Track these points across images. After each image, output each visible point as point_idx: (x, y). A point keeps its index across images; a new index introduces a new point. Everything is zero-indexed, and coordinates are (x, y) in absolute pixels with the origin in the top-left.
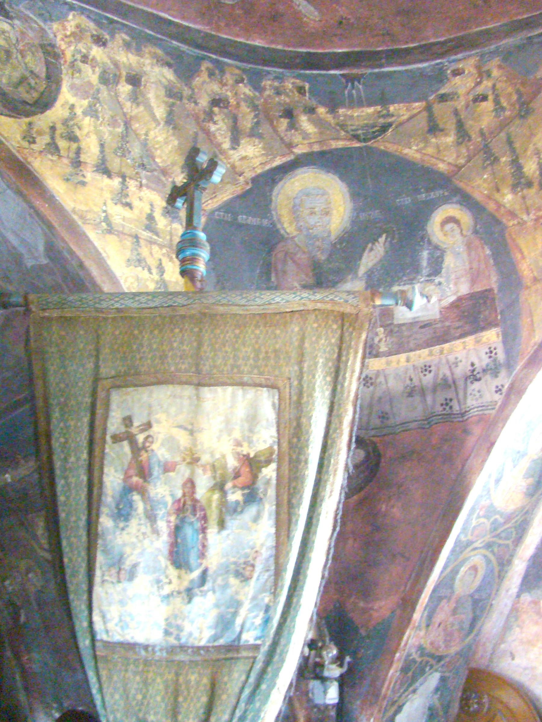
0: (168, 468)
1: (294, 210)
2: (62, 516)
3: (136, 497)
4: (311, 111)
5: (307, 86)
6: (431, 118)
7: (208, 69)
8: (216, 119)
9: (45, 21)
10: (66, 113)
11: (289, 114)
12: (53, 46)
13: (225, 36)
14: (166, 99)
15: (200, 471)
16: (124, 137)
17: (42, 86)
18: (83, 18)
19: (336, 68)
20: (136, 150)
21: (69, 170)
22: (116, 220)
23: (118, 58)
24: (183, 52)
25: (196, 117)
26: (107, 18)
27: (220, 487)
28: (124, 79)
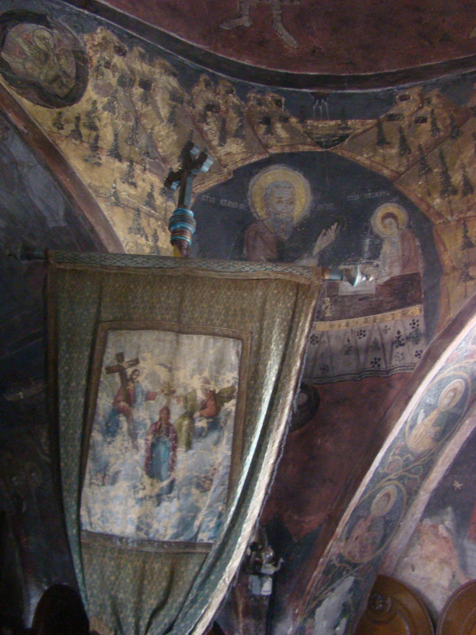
0: (149, 397)
1: (266, 199)
2: (63, 428)
3: (122, 418)
4: (285, 120)
5: (283, 100)
7: (205, 80)
8: (208, 120)
9: (78, 32)
10: (89, 107)
11: (267, 121)
12: (83, 53)
13: (221, 55)
14: (170, 102)
15: (174, 401)
16: (134, 130)
17: (72, 84)
18: (109, 32)
19: (308, 87)
20: (143, 141)
21: (88, 153)
22: (123, 195)
23: (134, 66)
24: (187, 65)
26: (128, 34)
27: (189, 415)
28: (137, 83)
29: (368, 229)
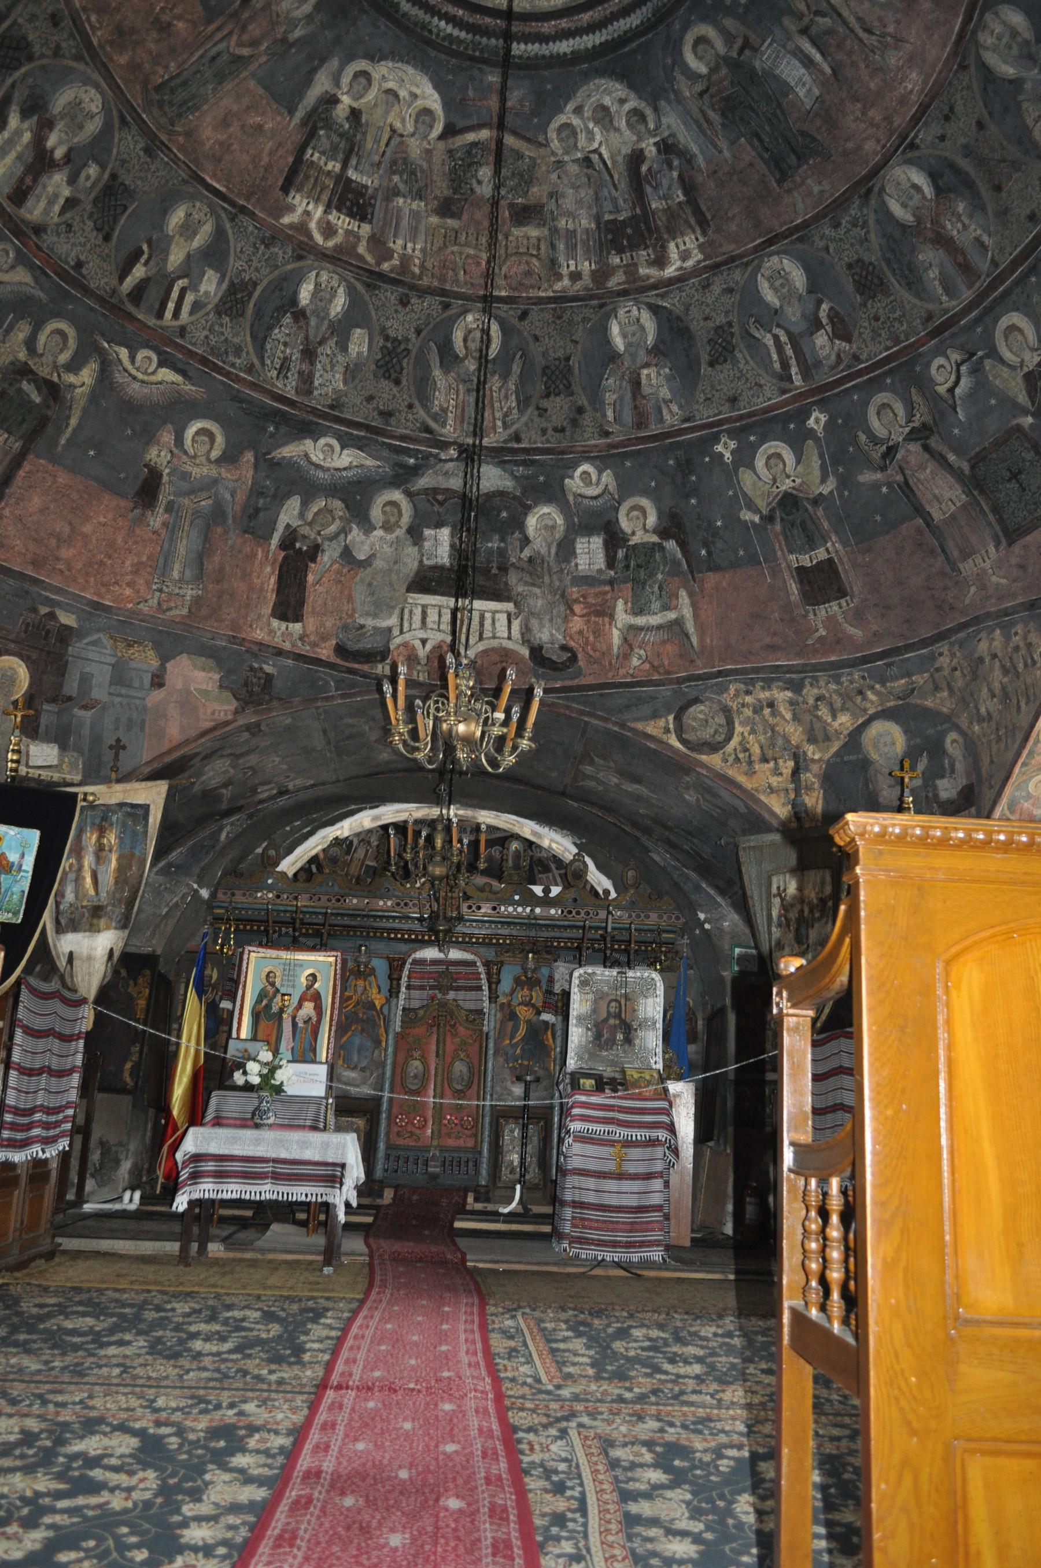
1: (876, 746)
4: (872, 688)
6: (934, 682)
11: (860, 692)
16: (772, 737)
20: (780, 742)
22: (775, 784)
29: (944, 752)
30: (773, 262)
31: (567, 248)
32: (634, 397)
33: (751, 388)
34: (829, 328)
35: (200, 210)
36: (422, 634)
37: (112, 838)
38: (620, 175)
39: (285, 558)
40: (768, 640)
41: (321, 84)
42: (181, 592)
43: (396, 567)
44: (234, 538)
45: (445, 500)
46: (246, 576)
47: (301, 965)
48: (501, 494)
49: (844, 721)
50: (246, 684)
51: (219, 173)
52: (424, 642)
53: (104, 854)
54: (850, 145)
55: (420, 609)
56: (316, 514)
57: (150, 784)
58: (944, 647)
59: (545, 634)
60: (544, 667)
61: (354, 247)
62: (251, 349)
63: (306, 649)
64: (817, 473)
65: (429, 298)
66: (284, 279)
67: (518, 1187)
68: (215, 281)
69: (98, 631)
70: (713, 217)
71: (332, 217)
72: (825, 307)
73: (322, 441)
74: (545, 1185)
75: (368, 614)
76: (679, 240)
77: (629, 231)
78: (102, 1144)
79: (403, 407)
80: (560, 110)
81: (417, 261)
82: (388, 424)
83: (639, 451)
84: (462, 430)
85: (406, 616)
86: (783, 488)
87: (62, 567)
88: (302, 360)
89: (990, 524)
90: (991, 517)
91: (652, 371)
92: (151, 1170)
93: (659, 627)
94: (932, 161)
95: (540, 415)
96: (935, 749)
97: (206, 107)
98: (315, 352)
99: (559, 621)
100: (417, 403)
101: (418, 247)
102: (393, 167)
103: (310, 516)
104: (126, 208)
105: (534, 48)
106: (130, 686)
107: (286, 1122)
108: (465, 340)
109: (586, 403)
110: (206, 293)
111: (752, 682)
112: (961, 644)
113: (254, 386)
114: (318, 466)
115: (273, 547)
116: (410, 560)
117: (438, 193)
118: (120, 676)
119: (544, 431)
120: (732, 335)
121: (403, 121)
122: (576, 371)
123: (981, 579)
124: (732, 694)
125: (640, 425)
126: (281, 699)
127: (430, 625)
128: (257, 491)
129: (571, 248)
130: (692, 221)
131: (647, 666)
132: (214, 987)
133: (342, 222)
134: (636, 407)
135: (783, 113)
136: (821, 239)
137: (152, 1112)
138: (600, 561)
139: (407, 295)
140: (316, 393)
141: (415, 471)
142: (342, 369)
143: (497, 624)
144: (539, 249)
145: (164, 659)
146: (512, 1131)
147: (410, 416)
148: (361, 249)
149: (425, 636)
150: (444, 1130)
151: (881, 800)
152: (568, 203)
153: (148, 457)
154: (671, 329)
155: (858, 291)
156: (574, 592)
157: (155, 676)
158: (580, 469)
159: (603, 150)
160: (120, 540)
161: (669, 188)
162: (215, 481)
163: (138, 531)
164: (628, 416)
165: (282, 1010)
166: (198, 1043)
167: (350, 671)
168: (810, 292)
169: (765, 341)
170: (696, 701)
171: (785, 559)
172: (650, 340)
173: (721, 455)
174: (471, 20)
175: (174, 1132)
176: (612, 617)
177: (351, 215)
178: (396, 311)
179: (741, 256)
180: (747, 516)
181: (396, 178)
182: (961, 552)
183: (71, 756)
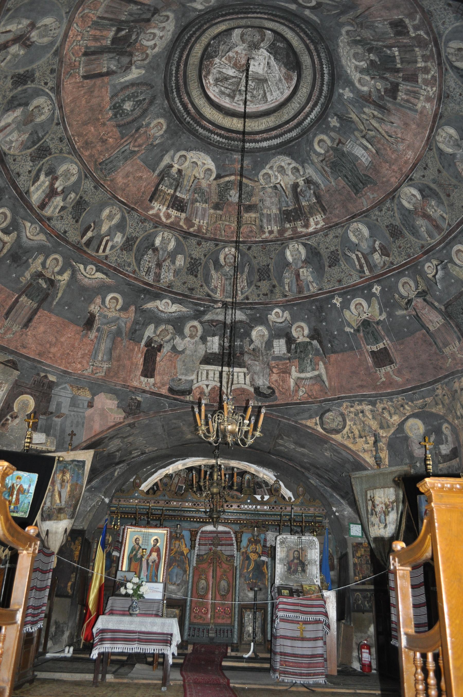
1: (411, 430)
4: (407, 404)
6: (435, 401)
11: (402, 406)
16: (364, 427)
20: (367, 428)
22: (366, 448)
25: (380, 414)
29: (442, 432)
30: (354, 225)
31: (267, 221)
32: (297, 281)
33: (347, 276)
34: (379, 251)
35: (115, 210)
36: (207, 383)
37: (68, 476)
38: (289, 192)
39: (147, 350)
40: (360, 383)
41: (166, 160)
42: (102, 366)
43: (195, 353)
44: (125, 342)
45: (217, 325)
46: (130, 358)
47: (151, 535)
48: (241, 322)
49: (396, 419)
50: (129, 406)
51: (124, 195)
52: (207, 386)
53: (64, 484)
54: (385, 179)
55: (205, 371)
56: (161, 331)
57: (86, 451)
58: (438, 385)
59: (261, 382)
60: (260, 396)
61: (179, 222)
62: (135, 264)
63: (155, 390)
64: (378, 311)
65: (210, 242)
66: (150, 235)
67: (252, 644)
68: (121, 237)
69: (65, 383)
70: (328, 208)
71: (170, 211)
72: (377, 242)
73: (164, 301)
74: (265, 642)
75: (183, 374)
76: (314, 217)
77: (293, 214)
78: (56, 623)
79: (198, 286)
80: (264, 168)
81: (205, 228)
82: (192, 293)
83: (300, 303)
84: (224, 295)
85: (200, 375)
86: (363, 318)
87: (51, 356)
88: (156, 268)
89: (455, 332)
90: (455, 329)
91: (304, 270)
92: (78, 636)
93: (311, 378)
94: (419, 185)
95: (257, 289)
96: (438, 431)
97: (119, 170)
98: (162, 263)
99: (267, 376)
100: (204, 284)
101: (205, 222)
102: (195, 192)
103: (158, 333)
104: (85, 209)
105: (252, 145)
106: (78, 407)
107: (144, 612)
108: (225, 259)
109: (276, 283)
110: (117, 242)
111: (353, 402)
112: (447, 384)
113: (136, 279)
114: (162, 311)
115: (142, 346)
116: (201, 351)
117: (214, 201)
118: (74, 402)
119: (259, 295)
120: (338, 254)
121: (199, 173)
122: (272, 271)
123: (453, 355)
124: (344, 407)
125: (300, 292)
126: (144, 412)
127: (210, 378)
128: (136, 322)
129: (269, 221)
130: (320, 210)
131: (306, 395)
132: (110, 545)
133: (174, 213)
134: (298, 285)
135: (356, 167)
136: (375, 215)
137: (79, 606)
138: (284, 350)
139: (200, 241)
140: (161, 281)
141: (204, 313)
142: (173, 271)
143: (240, 378)
144: (255, 221)
145: (94, 395)
146: (249, 615)
147: (201, 290)
148: (182, 223)
149: (208, 383)
150: (216, 615)
151: (415, 454)
152: (267, 203)
153: (90, 309)
154: (312, 253)
155: (391, 236)
156: (273, 363)
157: (89, 402)
158: (275, 311)
159: (282, 183)
160: (76, 344)
161: (310, 197)
162: (118, 319)
163: (84, 340)
164: (295, 288)
165: (142, 557)
166: (102, 573)
167: (175, 399)
168: (371, 237)
169: (352, 257)
170: (329, 410)
171: (366, 348)
172: (303, 257)
173: (336, 304)
174: (227, 135)
175: (90, 617)
176: (290, 374)
177: (178, 210)
178: (196, 247)
179: (341, 223)
180: (347, 329)
181: (196, 195)
182: (443, 344)
183: (51, 438)
